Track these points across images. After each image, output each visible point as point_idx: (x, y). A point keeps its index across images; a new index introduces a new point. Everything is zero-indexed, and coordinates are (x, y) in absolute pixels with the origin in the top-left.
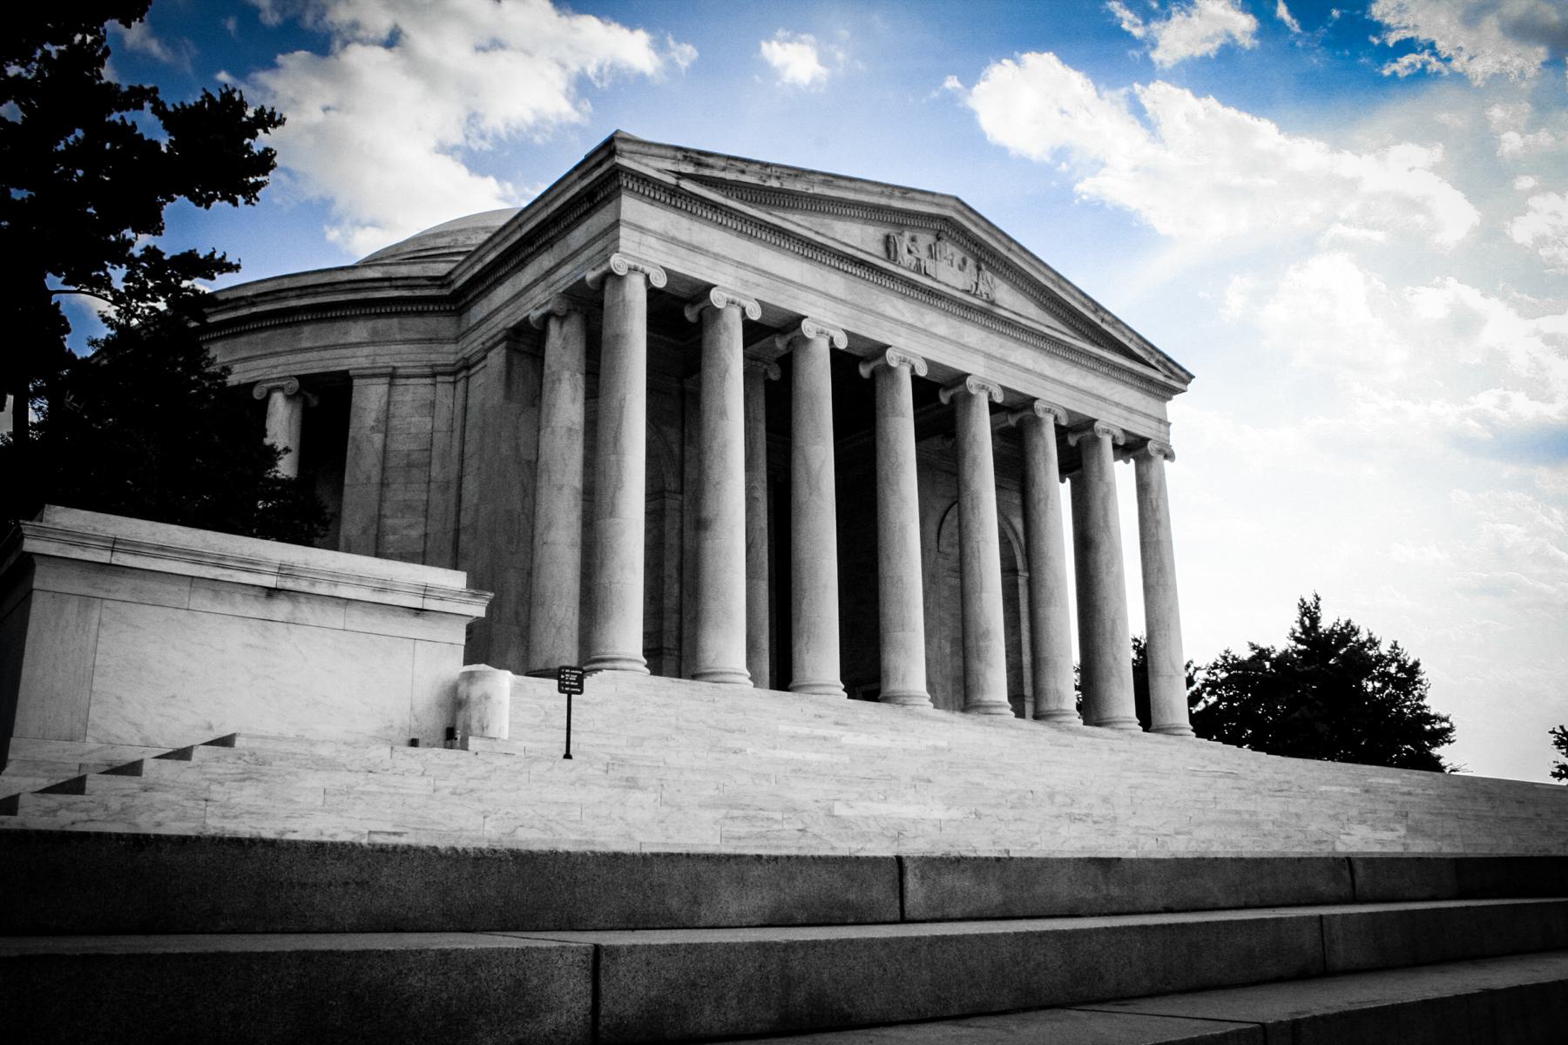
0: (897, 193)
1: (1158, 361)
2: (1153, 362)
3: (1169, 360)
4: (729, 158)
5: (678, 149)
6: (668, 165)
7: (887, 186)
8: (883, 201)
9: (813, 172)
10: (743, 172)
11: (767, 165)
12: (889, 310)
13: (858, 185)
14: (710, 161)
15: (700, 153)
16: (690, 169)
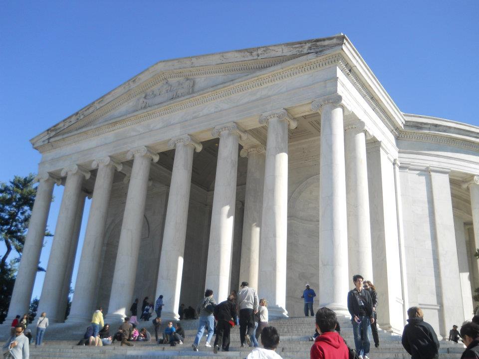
0: (131, 83)
1: (310, 48)
2: (305, 51)
3: (318, 41)
4: (64, 121)
5: (48, 130)
6: (47, 137)
7: (125, 83)
8: (126, 90)
9: (94, 103)
10: (71, 122)
11: (77, 113)
12: (133, 134)
13: (113, 92)
14: (59, 126)
15: (54, 126)
16: (53, 134)
